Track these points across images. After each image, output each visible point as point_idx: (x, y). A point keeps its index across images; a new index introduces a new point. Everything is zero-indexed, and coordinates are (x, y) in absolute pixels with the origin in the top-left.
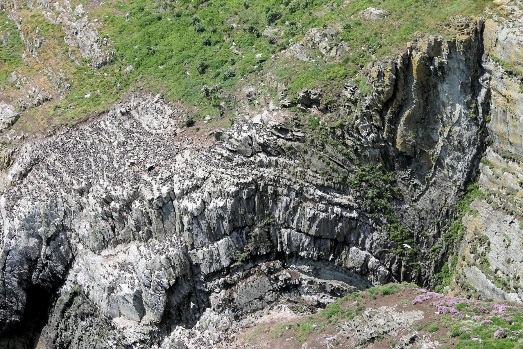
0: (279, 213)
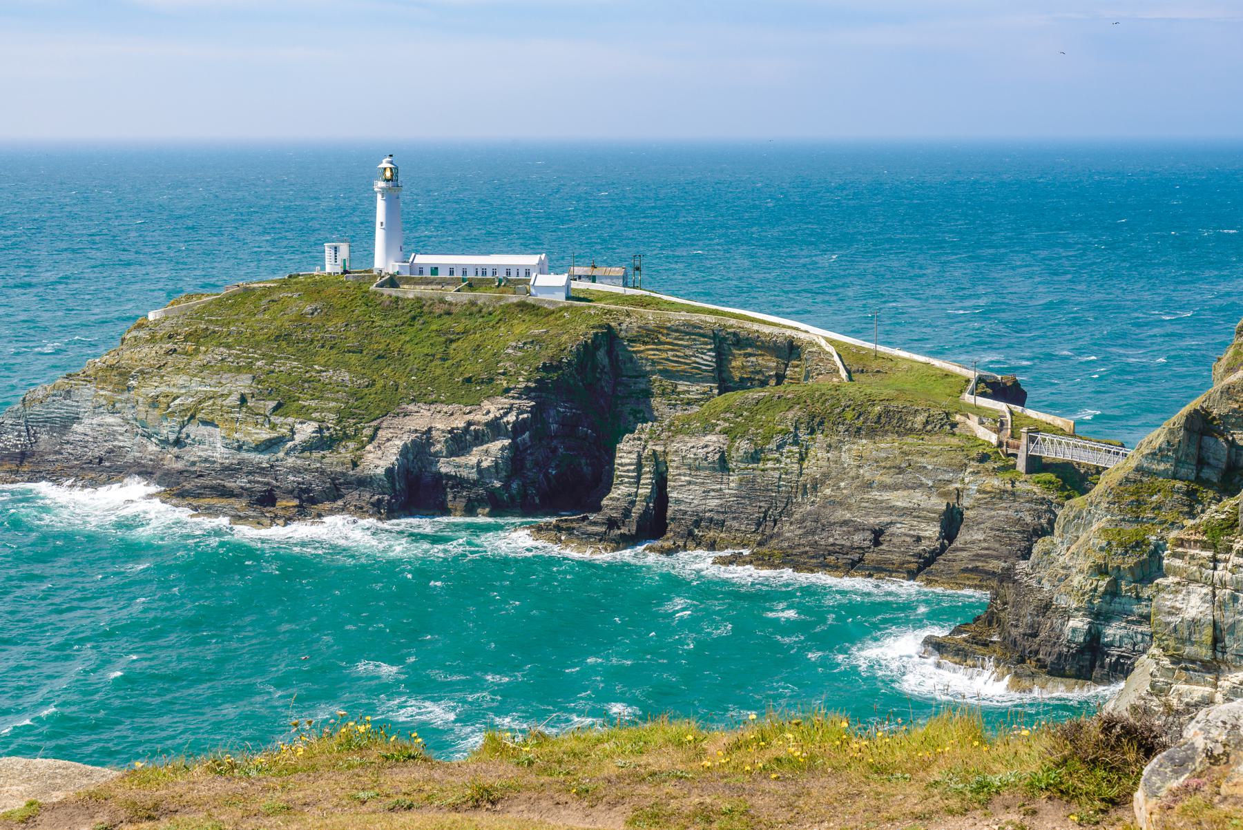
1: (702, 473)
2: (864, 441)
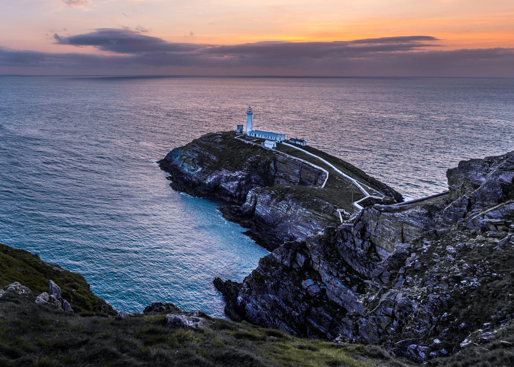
2: (305, 209)
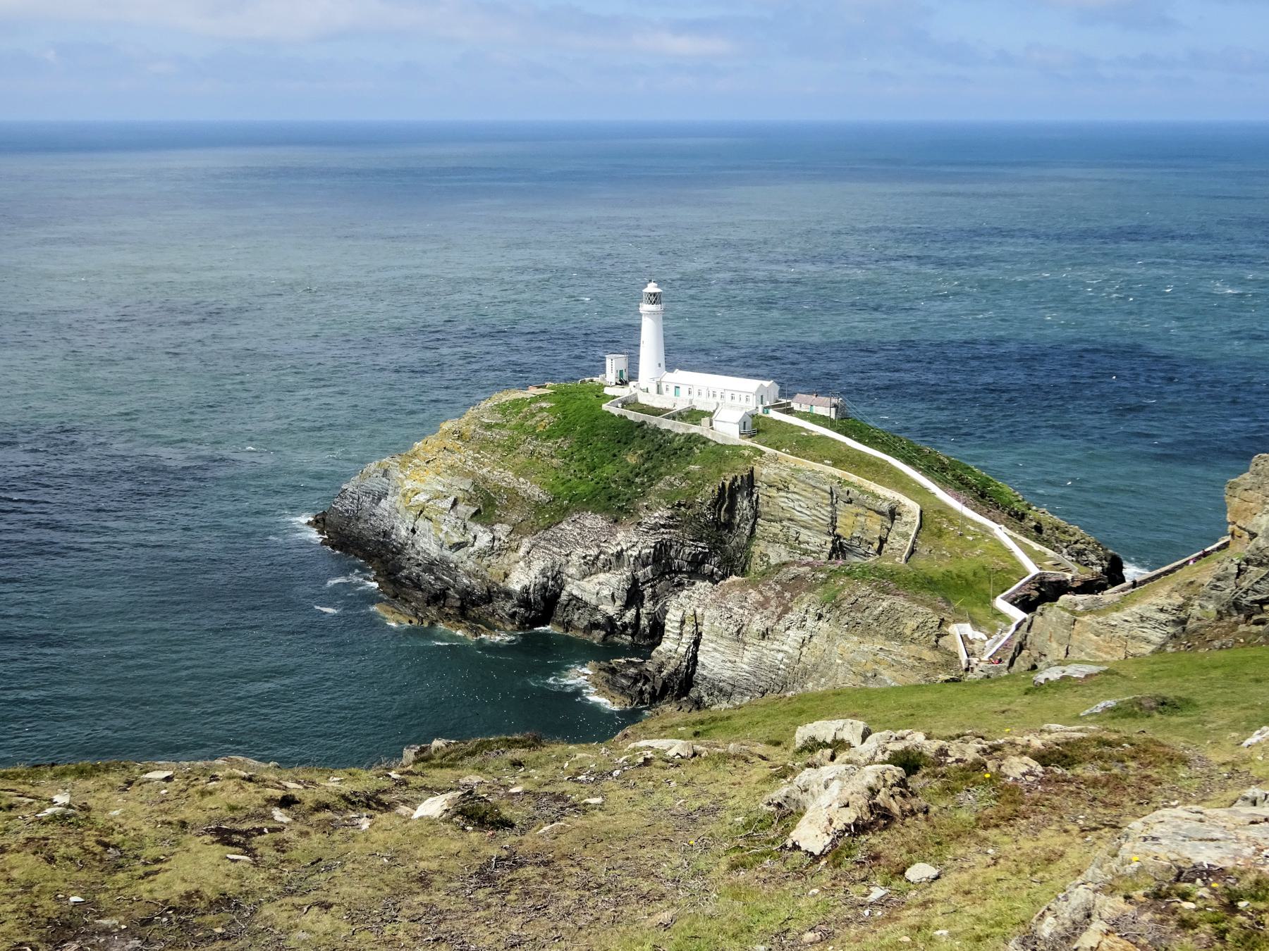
0: (672, 553)
1: (725, 642)
2: (856, 638)
